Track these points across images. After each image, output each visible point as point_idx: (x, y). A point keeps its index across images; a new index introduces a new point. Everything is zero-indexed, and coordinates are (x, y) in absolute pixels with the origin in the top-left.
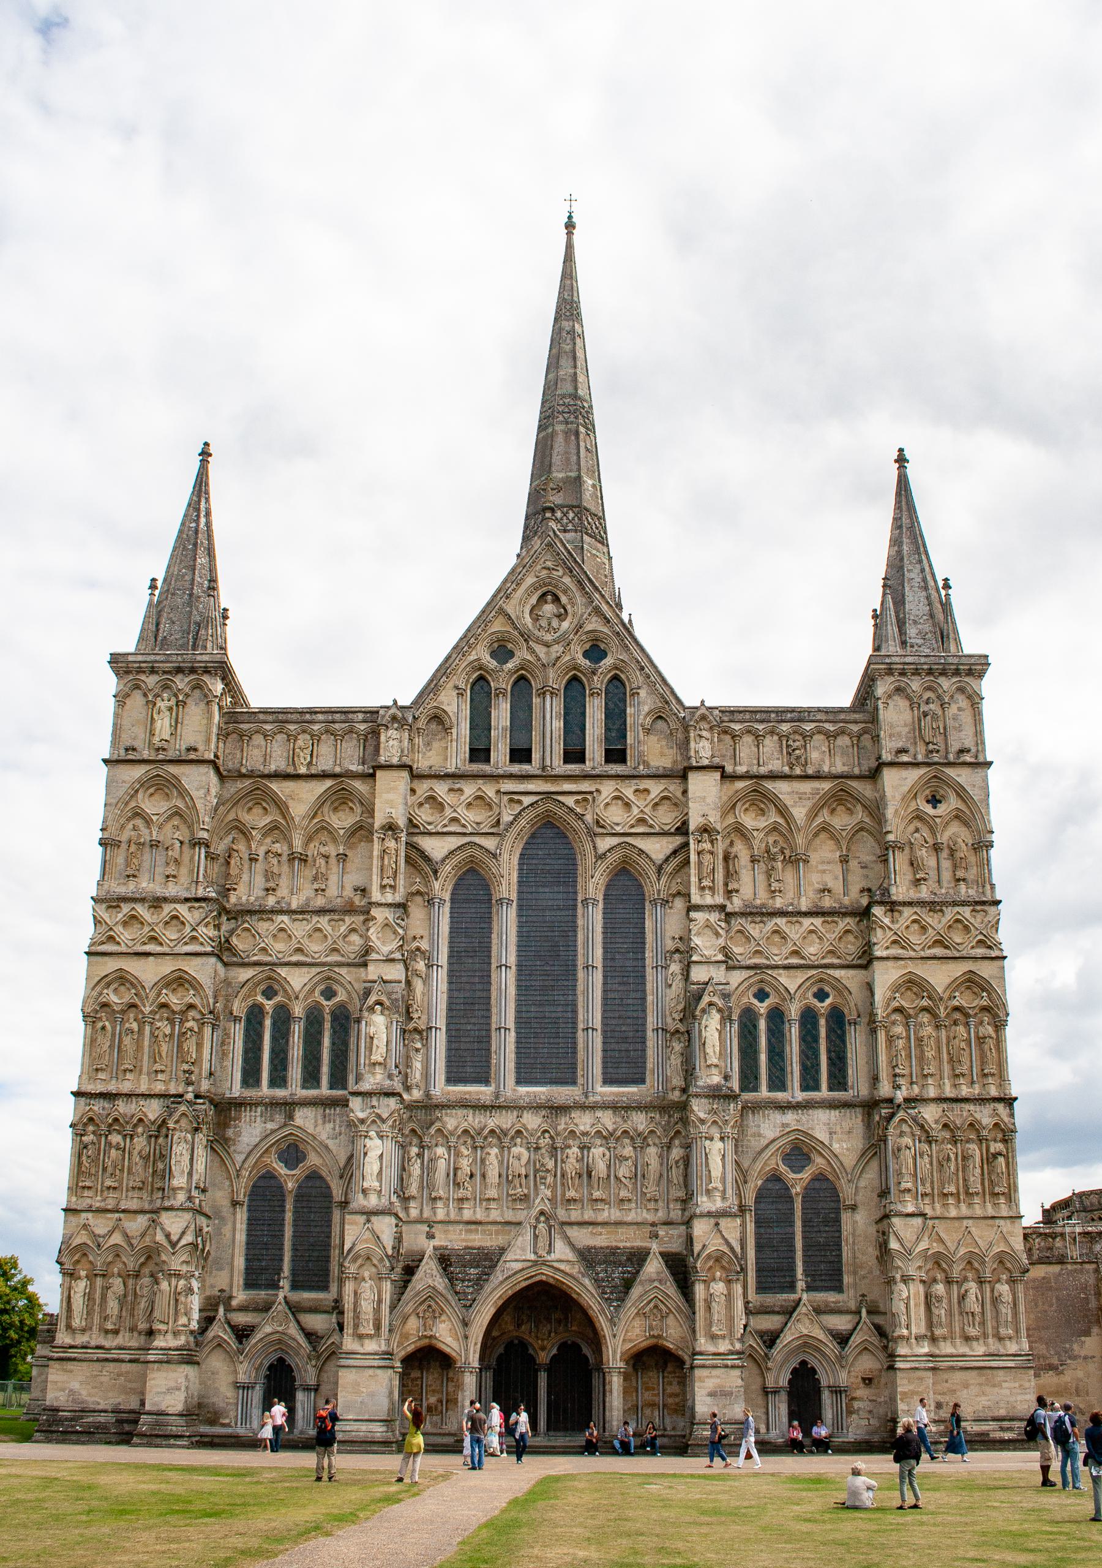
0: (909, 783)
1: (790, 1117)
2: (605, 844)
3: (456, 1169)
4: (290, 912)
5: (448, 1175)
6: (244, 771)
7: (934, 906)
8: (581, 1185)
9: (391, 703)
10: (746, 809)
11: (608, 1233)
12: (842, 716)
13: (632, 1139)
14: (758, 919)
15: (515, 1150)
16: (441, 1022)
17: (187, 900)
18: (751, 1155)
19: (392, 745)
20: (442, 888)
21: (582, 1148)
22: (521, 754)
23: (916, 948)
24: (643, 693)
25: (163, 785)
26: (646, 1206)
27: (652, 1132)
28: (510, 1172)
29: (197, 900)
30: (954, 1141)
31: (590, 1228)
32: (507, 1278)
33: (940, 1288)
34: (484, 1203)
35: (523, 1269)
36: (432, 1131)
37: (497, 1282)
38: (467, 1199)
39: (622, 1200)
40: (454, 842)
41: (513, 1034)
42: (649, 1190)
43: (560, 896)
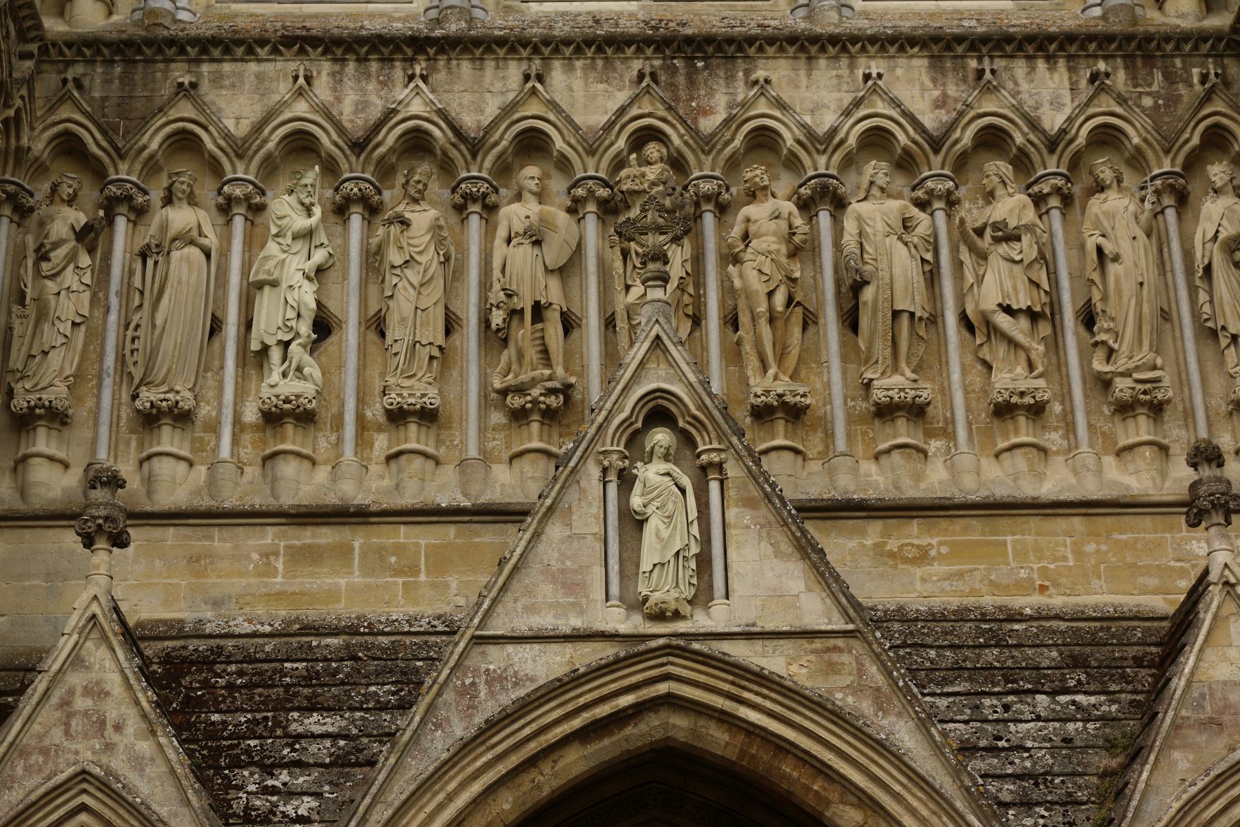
3: (252, 290)
5: (216, 327)
8: (811, 356)
11: (957, 551)
13: (1021, 162)
15: (515, 214)
21: (806, 206)
26: (1109, 438)
27: (1106, 137)
28: (497, 295)
31: (874, 530)
32: (492, 726)
34: (381, 443)
35: (574, 680)
36: (154, 140)
37: (439, 745)
38: (306, 418)
39: (1004, 411)
42: (1121, 364)
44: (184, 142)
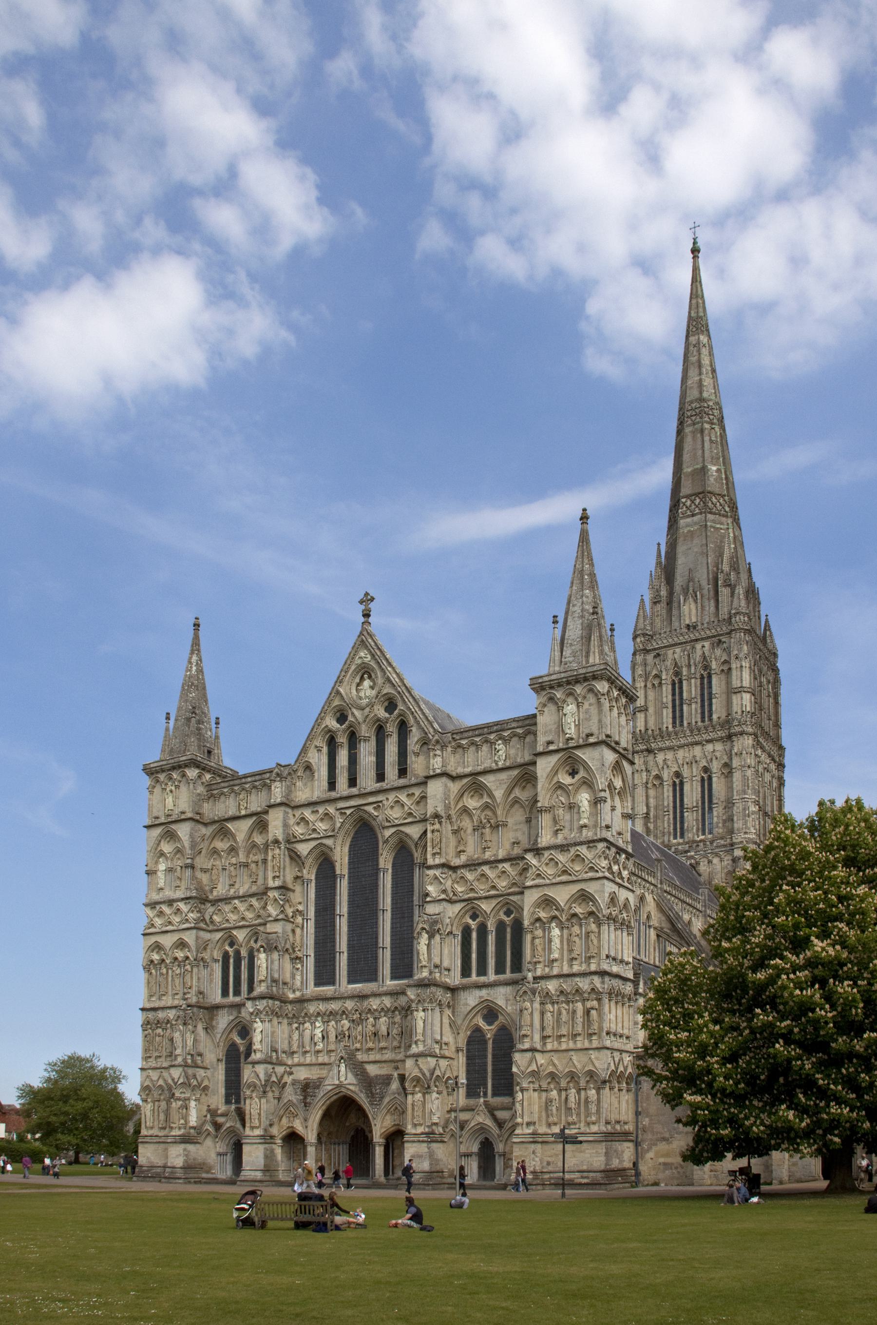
0: (552, 764)
1: (484, 993)
2: (388, 833)
4: (238, 897)
6: (216, 818)
7: (563, 848)
9: (274, 766)
10: (472, 796)
12: (527, 722)
14: (473, 868)
16: (311, 952)
17: (183, 899)
18: (462, 1017)
19: (278, 792)
20: (310, 874)
22: (352, 782)
23: (550, 877)
24: (414, 729)
25: (171, 836)
29: (187, 898)
30: (568, 1003)
31: (379, 1065)
33: (554, 1093)
40: (313, 844)
41: (346, 954)
43: (370, 868)
44: (306, 1014)
